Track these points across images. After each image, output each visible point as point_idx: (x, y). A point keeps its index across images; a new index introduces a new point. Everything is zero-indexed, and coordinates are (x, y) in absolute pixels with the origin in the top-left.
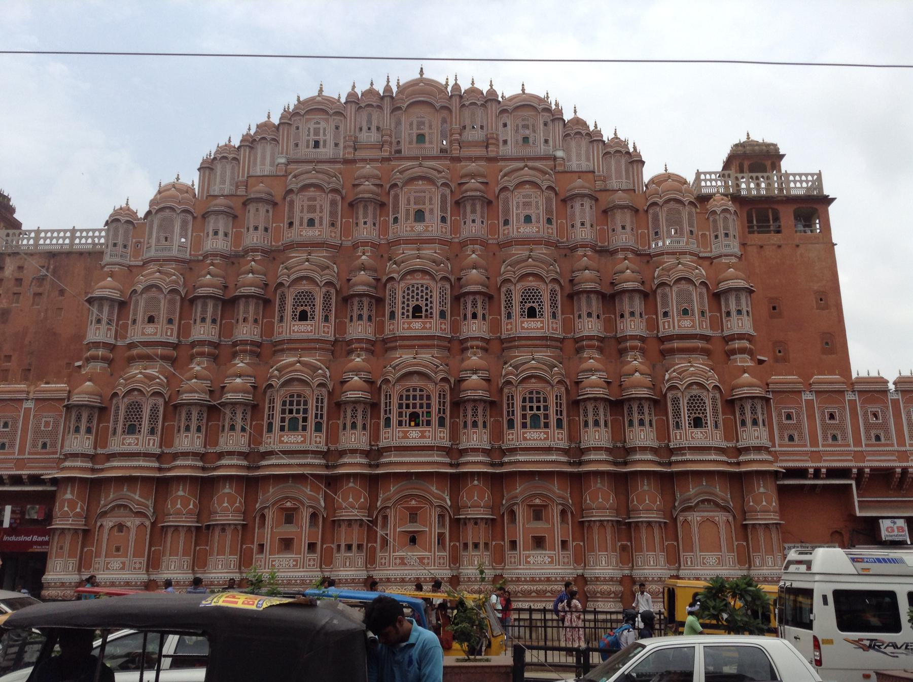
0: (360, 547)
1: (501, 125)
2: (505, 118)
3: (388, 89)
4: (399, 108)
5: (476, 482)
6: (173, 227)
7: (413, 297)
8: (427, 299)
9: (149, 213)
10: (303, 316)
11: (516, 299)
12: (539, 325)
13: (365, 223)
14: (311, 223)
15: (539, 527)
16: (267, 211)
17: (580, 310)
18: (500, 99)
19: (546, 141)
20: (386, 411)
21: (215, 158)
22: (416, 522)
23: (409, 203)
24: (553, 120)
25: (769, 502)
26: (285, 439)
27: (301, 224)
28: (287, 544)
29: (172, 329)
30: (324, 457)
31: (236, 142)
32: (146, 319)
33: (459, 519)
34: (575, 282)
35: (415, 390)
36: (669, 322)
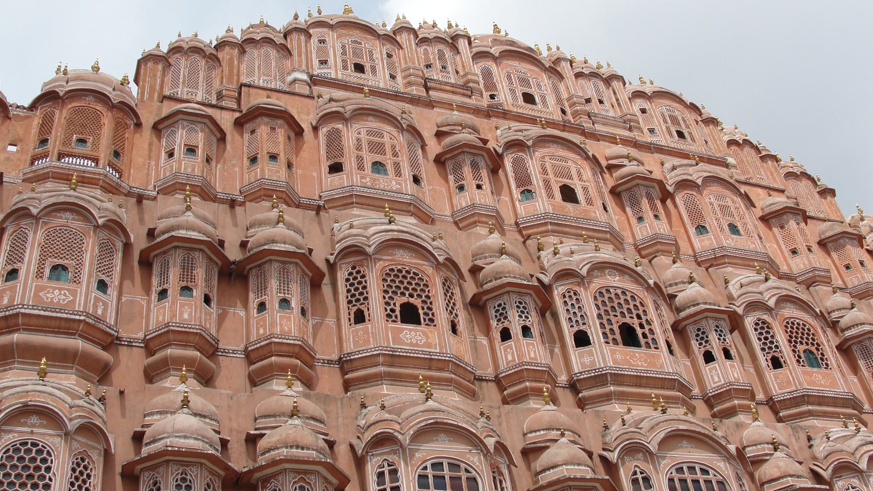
2: (640, 103)
9: (49, 97)
16: (289, 138)
21: (175, 49)
23: (545, 171)
29: (105, 304)
32: (47, 271)
34: (844, 322)
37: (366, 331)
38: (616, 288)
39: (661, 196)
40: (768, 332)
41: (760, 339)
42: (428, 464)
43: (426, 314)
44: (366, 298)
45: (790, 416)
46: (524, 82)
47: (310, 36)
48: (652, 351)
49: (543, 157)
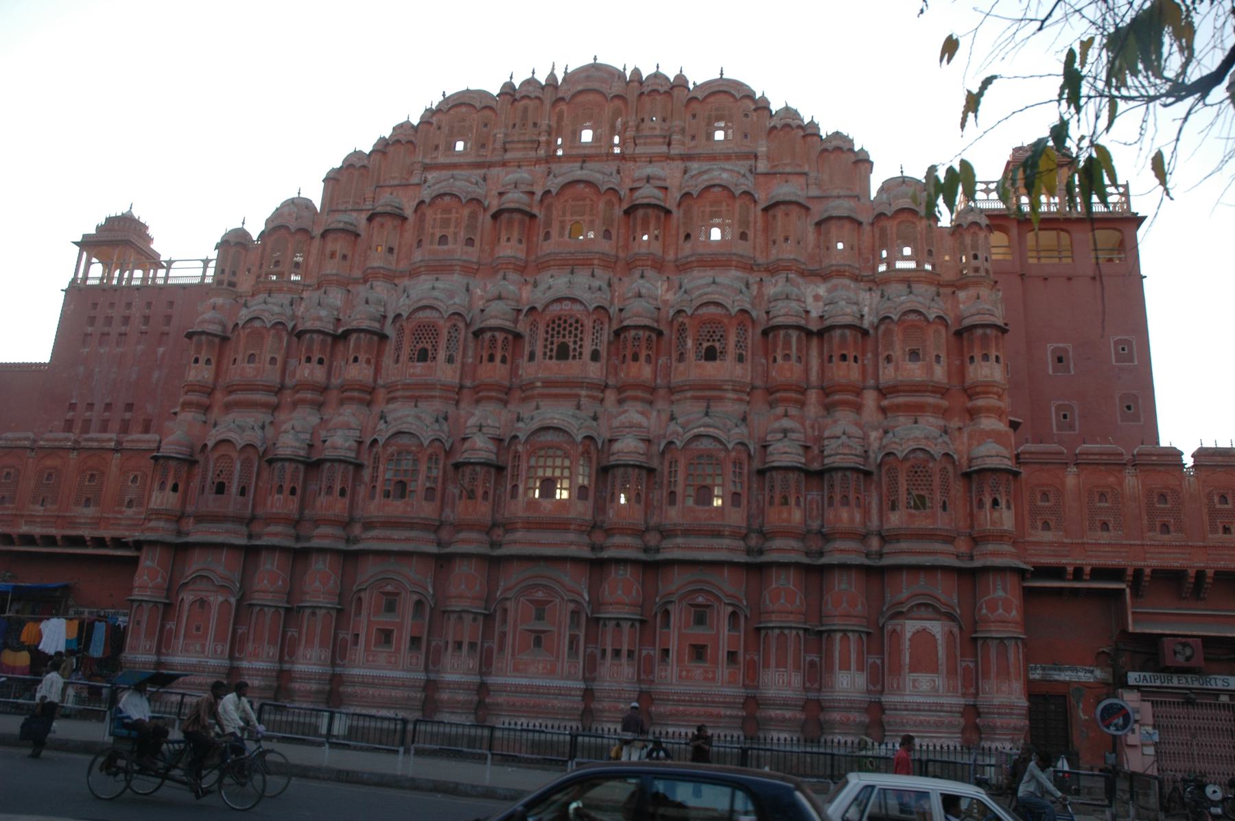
0: (472, 645)
1: (689, 117)
3: (552, 76)
4: (562, 99)
8: (576, 336)
9: (263, 233)
10: (423, 356)
13: (508, 240)
14: (443, 240)
15: (699, 633)
17: (774, 351)
18: (691, 86)
24: (755, 110)
25: (1008, 609)
28: (386, 636)
30: (435, 532)
31: (367, 150)
33: (598, 619)
47: (430, 123)
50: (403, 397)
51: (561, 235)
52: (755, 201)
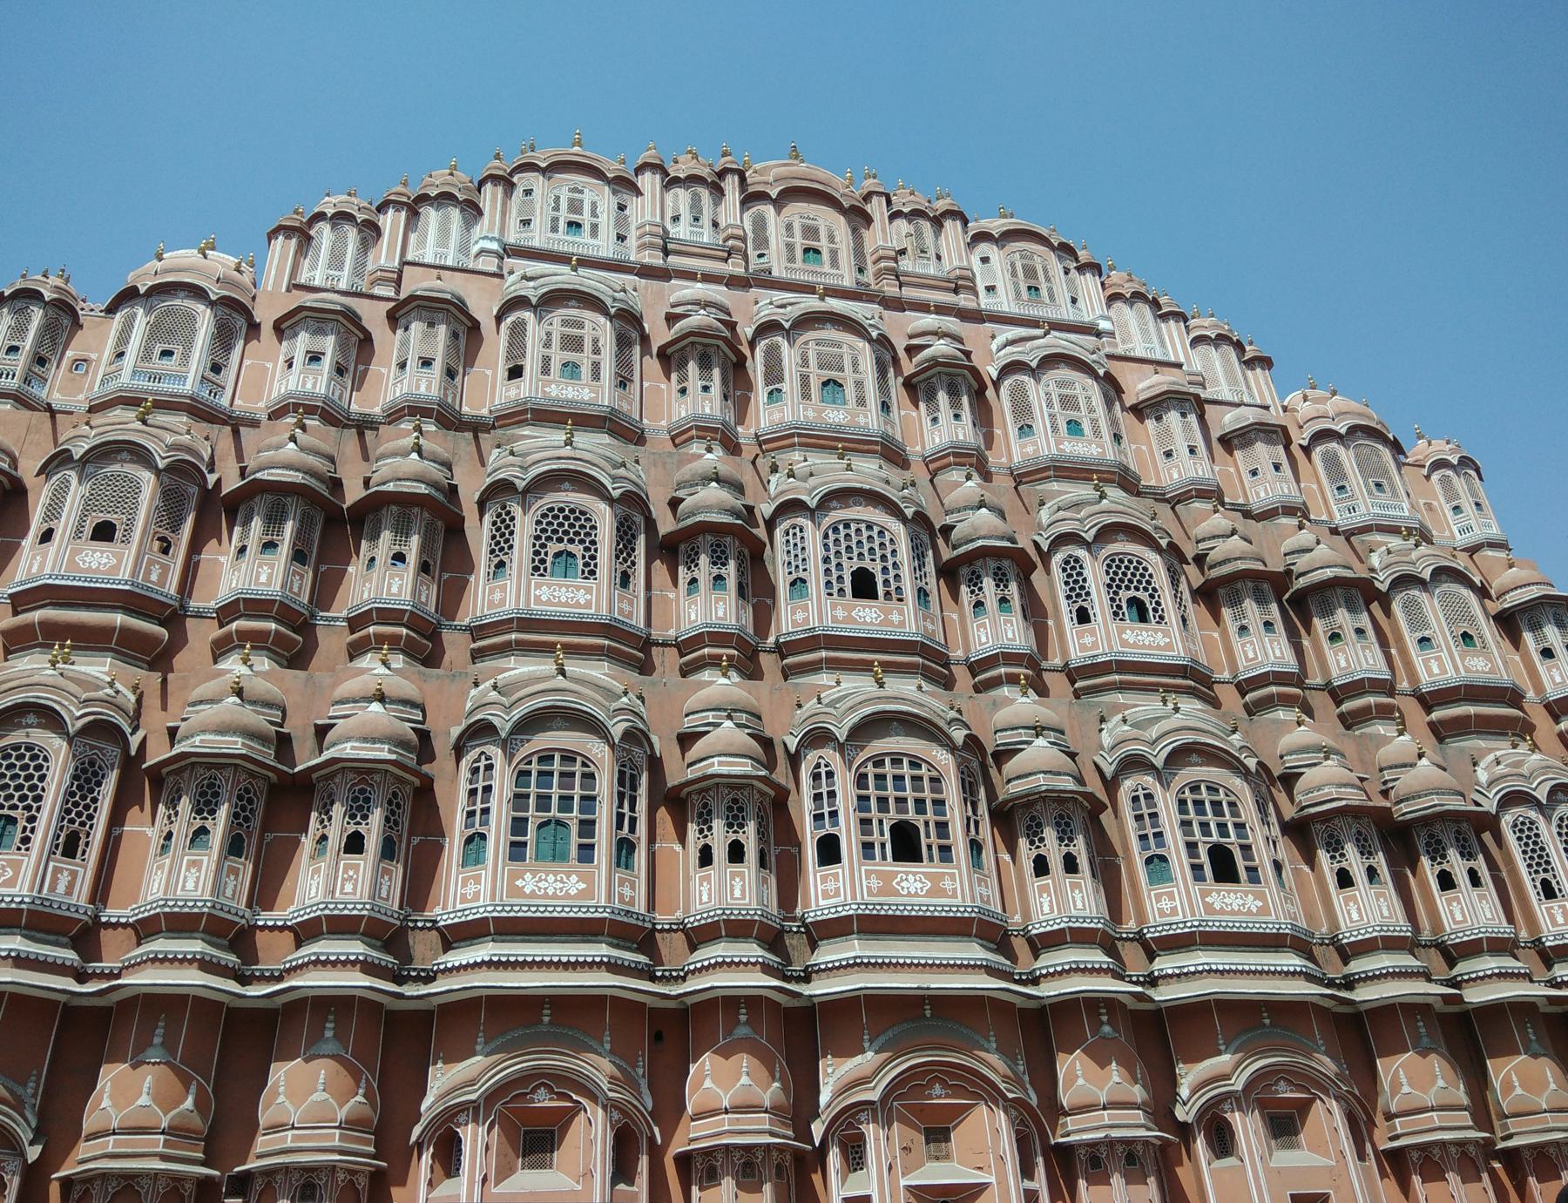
2: (984, 248)
5: (1107, 1029)
6: (194, 332)
7: (849, 548)
8: (884, 558)
11: (1094, 574)
12: (1161, 639)
13: (706, 389)
14: (571, 369)
19: (1074, 301)
20: (818, 818)
22: (947, 1157)
26: (528, 883)
27: (546, 370)
29: (165, 569)
32: (88, 530)
34: (1213, 556)
35: (897, 762)
36: (1438, 659)
37: (503, 589)
38: (858, 521)
39: (975, 385)
40: (1079, 574)
41: (1067, 583)
42: (535, 759)
43: (586, 565)
44: (511, 547)
45: (1088, 687)
46: (811, 232)
47: (513, 185)
48: (894, 604)
49: (806, 343)
50: (519, 643)
51: (806, 395)
52: (1119, 390)
